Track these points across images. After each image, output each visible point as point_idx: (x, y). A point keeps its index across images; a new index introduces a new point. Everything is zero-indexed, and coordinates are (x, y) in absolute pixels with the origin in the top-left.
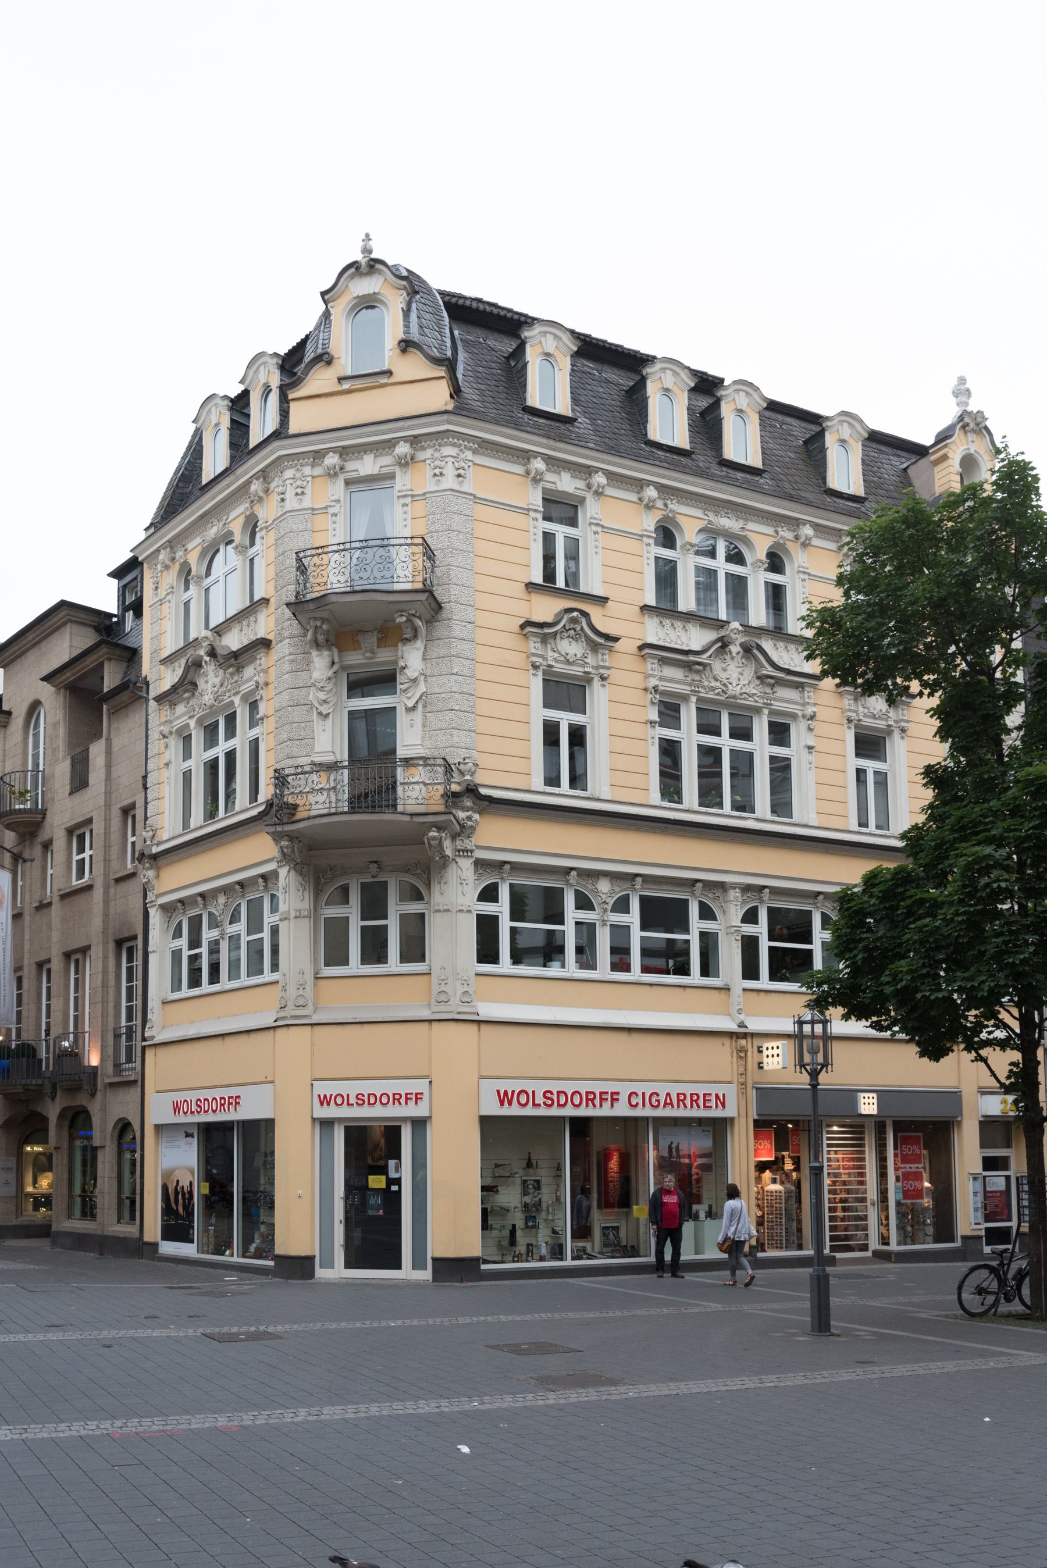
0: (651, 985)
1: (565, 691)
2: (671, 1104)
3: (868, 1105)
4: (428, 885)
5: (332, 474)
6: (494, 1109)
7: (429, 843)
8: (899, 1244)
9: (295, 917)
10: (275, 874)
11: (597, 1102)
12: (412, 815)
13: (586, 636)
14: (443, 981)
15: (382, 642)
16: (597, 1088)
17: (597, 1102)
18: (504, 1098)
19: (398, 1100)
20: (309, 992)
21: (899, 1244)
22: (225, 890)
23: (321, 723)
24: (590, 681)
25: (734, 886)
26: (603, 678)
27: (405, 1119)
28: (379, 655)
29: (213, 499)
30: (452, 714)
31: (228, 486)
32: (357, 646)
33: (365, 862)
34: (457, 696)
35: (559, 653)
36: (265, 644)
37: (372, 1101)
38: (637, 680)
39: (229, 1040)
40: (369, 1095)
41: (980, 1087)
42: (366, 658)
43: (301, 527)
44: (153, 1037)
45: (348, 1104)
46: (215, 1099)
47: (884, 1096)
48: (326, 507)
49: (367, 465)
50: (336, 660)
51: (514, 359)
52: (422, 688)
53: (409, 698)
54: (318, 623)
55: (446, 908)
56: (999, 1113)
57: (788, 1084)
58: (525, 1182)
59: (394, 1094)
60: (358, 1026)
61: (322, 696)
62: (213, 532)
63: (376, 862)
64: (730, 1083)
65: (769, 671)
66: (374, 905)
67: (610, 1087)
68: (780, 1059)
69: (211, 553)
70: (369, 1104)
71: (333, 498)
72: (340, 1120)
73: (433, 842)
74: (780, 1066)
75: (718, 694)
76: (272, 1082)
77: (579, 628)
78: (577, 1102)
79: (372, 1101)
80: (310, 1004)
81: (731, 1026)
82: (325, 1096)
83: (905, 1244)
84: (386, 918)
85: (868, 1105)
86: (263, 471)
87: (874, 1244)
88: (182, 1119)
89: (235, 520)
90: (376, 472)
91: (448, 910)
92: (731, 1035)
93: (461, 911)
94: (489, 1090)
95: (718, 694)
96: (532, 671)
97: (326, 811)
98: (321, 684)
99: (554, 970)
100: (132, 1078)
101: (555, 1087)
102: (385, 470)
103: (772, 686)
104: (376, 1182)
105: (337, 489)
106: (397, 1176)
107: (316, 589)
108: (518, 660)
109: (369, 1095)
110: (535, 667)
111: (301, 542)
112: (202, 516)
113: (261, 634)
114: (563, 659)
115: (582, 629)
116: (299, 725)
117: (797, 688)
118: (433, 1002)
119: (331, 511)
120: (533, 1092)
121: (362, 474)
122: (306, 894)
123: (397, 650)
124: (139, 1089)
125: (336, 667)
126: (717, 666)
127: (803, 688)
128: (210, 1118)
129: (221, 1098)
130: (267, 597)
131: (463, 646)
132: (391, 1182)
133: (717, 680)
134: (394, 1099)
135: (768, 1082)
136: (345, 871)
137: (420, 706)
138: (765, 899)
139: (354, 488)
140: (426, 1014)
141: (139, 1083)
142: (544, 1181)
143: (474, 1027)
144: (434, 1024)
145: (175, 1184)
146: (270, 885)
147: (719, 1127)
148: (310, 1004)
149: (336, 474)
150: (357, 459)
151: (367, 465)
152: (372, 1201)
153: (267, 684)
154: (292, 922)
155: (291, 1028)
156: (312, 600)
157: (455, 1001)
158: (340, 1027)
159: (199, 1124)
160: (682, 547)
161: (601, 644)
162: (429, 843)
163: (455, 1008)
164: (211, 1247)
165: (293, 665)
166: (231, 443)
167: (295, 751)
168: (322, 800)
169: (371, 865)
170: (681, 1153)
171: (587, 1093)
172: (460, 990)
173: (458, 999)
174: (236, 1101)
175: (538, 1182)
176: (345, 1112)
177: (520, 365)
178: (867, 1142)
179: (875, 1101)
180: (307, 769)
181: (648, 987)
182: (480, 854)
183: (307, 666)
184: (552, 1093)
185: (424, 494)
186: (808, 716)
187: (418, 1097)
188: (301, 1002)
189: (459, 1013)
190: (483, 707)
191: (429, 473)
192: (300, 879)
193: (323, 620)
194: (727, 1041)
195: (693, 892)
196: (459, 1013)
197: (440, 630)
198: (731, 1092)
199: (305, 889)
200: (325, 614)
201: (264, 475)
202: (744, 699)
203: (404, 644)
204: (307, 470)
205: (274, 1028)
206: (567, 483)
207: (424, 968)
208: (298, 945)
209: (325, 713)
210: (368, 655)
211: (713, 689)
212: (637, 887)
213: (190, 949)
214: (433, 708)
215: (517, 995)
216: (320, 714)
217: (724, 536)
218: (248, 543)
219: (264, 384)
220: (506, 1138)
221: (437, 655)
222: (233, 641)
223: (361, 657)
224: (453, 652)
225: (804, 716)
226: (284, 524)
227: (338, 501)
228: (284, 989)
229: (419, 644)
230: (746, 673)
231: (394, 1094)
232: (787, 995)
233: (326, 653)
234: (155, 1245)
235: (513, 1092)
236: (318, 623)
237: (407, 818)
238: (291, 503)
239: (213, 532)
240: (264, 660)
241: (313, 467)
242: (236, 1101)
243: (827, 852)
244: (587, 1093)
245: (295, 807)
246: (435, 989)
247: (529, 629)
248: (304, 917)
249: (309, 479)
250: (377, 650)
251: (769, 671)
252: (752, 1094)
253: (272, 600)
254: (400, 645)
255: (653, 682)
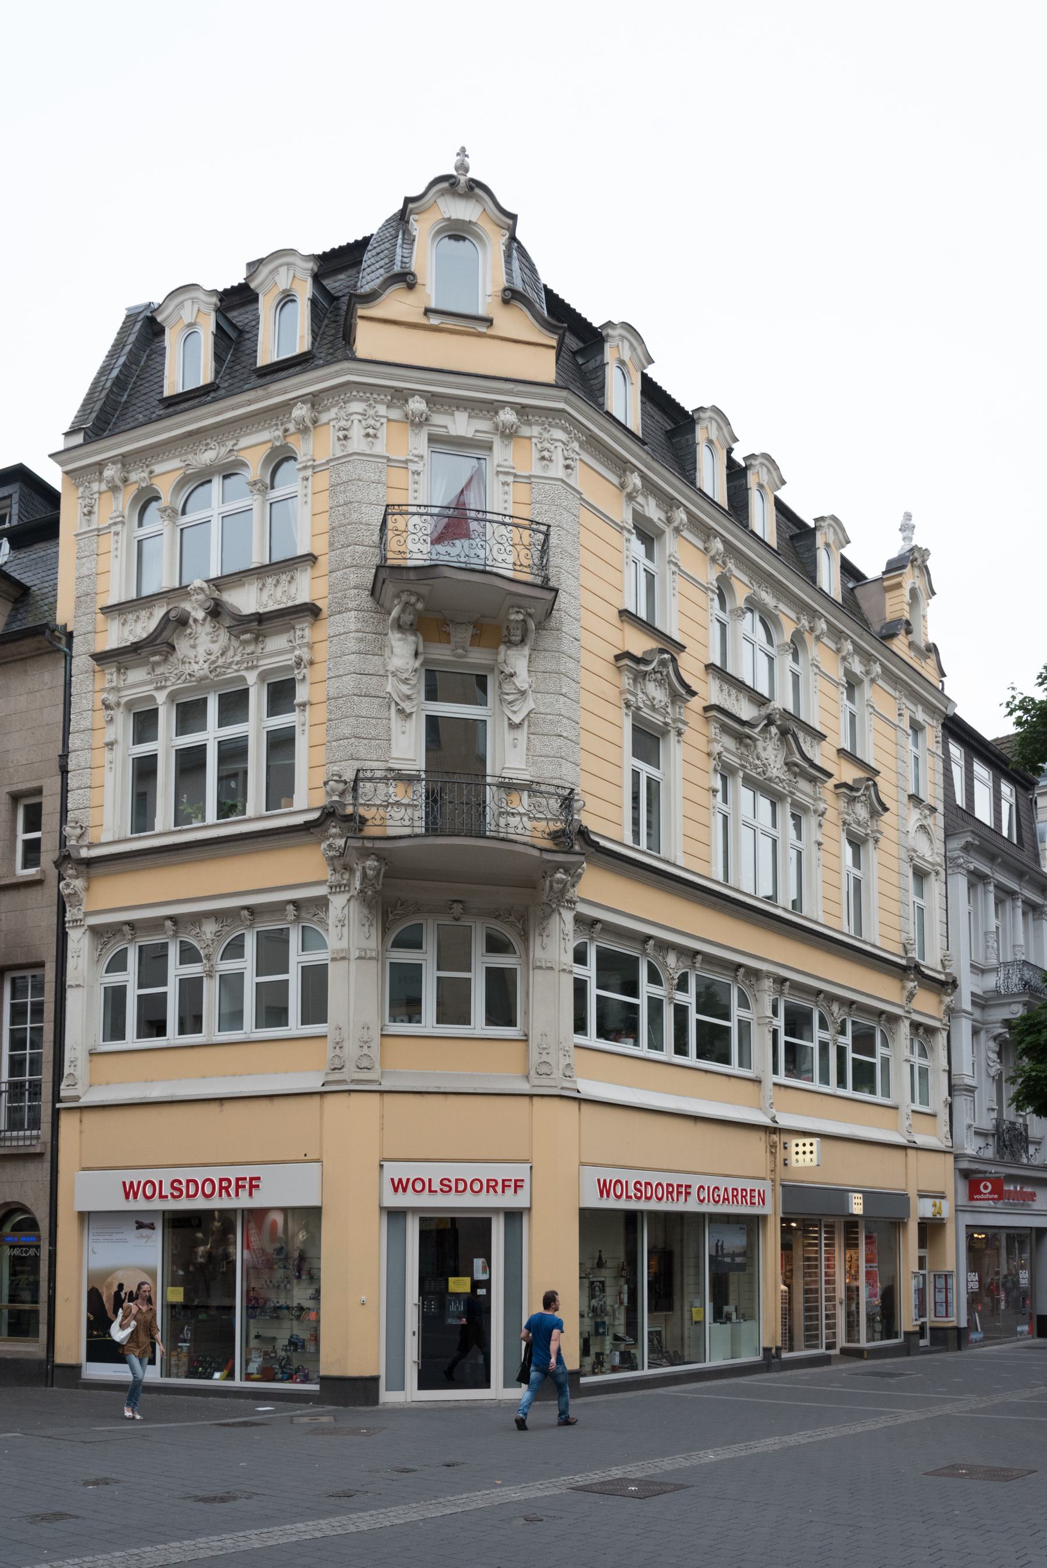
0: (706, 1071)
1: (648, 741)
2: (728, 1199)
3: (857, 1206)
4: (525, 937)
5: (417, 422)
6: (593, 1201)
7: (551, 887)
8: (868, 1341)
9: (360, 958)
10: (322, 903)
11: (232, 1190)
12: (541, 850)
13: (671, 685)
14: (543, 1050)
15: (476, 640)
16: (232, 1173)
17: (232, 1190)
18: (604, 1189)
19: (494, 1187)
20: (375, 1052)
21: (868, 1341)
22: (217, 915)
23: (400, 723)
24: (665, 733)
25: (768, 975)
26: (680, 733)
27: (496, 1210)
28: (471, 655)
29: (218, 414)
30: (559, 741)
31: (250, 403)
32: (445, 638)
33: (460, 898)
34: (565, 721)
35: (647, 696)
36: (311, 611)
37: (461, 1187)
38: (700, 742)
39: (228, 1107)
40: (457, 1180)
41: (919, 1191)
42: (454, 656)
43: (374, 477)
44: (77, 1098)
45: (430, 1191)
46: (650, 1184)
47: (869, 1197)
48: (406, 462)
49: (461, 425)
50: (421, 650)
51: (582, 356)
52: (530, 704)
53: (515, 712)
54: (413, 599)
55: (549, 965)
56: (931, 1216)
57: (803, 1182)
58: (592, 1283)
59: (488, 1181)
60: (441, 1098)
61: (405, 689)
62: (207, 456)
63: (460, 901)
64: (764, 1179)
65: (797, 758)
66: (455, 955)
67: (684, 1180)
68: (814, 1156)
69: (202, 479)
70: (457, 1191)
71: (416, 452)
72: (415, 1210)
73: (555, 885)
74: (814, 1163)
75: (759, 774)
76: (582, 1164)
77: (665, 673)
78: (208, 1191)
79: (461, 1187)
80: (377, 1066)
81: (765, 1121)
82: (400, 1181)
83: (873, 1340)
84: (287, 972)
85: (857, 1206)
86: (314, 395)
87: (841, 1341)
88: (132, 1205)
89: (254, 448)
90: (470, 435)
91: (551, 968)
92: (765, 1129)
93: (564, 970)
94: (591, 1177)
95: (759, 774)
96: (625, 710)
97: (407, 831)
98: (405, 676)
99: (625, 1047)
100: (38, 1150)
101: (183, 1174)
102: (481, 436)
103: (795, 775)
104: (459, 1285)
105: (419, 443)
106: (485, 1277)
107: (415, 556)
108: (612, 693)
109: (457, 1180)
110: (628, 706)
111: (395, 498)
112: (190, 434)
113: (303, 598)
114: (649, 703)
115: (668, 675)
116: (357, 721)
117: (810, 781)
118: (532, 1073)
119: (412, 467)
120: (430, 1180)
121: (453, 433)
122: (373, 930)
123: (497, 654)
124: (47, 1166)
125: (421, 658)
126: (760, 744)
127: (816, 782)
128: (184, 1204)
129: (668, 1185)
130: (316, 554)
131: (571, 665)
132: (476, 1285)
133: (758, 759)
134: (488, 1186)
135: (793, 1177)
136: (418, 909)
137: (526, 724)
138: (786, 991)
139: (438, 447)
140: (525, 1087)
141: (48, 1157)
142: (607, 1284)
143: (574, 1106)
144: (535, 1100)
145: (115, 1289)
146: (304, 915)
147: (752, 1224)
148: (377, 1066)
149: (420, 425)
150: (446, 413)
151: (461, 425)
152: (453, 1308)
153: (311, 663)
154: (353, 965)
155: (353, 1095)
156: (415, 568)
157: (557, 1074)
158: (418, 1097)
159: (164, 1212)
160: (731, 612)
161: (681, 696)
162: (551, 887)
163: (556, 1083)
164: (184, 1368)
165: (362, 645)
166: (215, 354)
167: (363, 753)
168: (399, 815)
169: (455, 905)
170: (725, 1252)
171: (221, 1180)
172: (564, 1062)
173: (561, 1072)
174: (254, 1184)
175: (603, 1283)
176: (425, 1201)
177: (591, 365)
178: (836, 1242)
179: (861, 1201)
180: (379, 774)
181: (703, 1074)
182: (582, 908)
183: (380, 649)
184: (180, 1183)
185: (529, 477)
186: (820, 812)
187: (518, 1185)
188: (365, 1063)
189: (562, 1088)
190: (586, 740)
191: (536, 455)
192: (366, 911)
193: (420, 597)
194: (762, 1135)
195: (735, 978)
196: (562, 1088)
197: (548, 640)
198: (765, 1186)
199: (371, 925)
200: (424, 590)
201: (315, 400)
202: (777, 784)
203: (508, 648)
204: (382, 409)
205: (321, 1094)
206: (653, 511)
207: (516, 1033)
208: (357, 993)
209: (408, 711)
210: (460, 651)
211: (756, 767)
212: (697, 965)
213: (140, 986)
214: (537, 730)
215: (612, 1075)
216: (401, 711)
217: (760, 611)
218: (268, 481)
219: (284, 291)
220: (609, 1232)
221: (542, 669)
222: (247, 600)
223: (448, 652)
224: (562, 668)
225: (815, 811)
226: (350, 467)
227: (422, 457)
228: (339, 1045)
229: (526, 651)
230: (779, 756)
231: (488, 1181)
232: (799, 1092)
233: (412, 638)
234: (77, 1369)
235: (408, 1180)
236: (413, 599)
237: (536, 853)
238: (357, 443)
239: (207, 456)
240: (305, 631)
241: (388, 407)
242: (254, 1184)
243: (829, 951)
244: (221, 1180)
245: (363, 821)
246: (535, 1058)
247: (626, 662)
248: (371, 958)
249: (384, 420)
250: (469, 648)
251: (797, 758)
252: (779, 1189)
253: (322, 560)
254: (502, 648)
255: (717, 748)
